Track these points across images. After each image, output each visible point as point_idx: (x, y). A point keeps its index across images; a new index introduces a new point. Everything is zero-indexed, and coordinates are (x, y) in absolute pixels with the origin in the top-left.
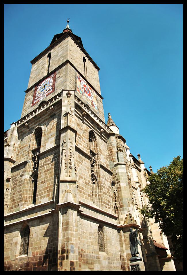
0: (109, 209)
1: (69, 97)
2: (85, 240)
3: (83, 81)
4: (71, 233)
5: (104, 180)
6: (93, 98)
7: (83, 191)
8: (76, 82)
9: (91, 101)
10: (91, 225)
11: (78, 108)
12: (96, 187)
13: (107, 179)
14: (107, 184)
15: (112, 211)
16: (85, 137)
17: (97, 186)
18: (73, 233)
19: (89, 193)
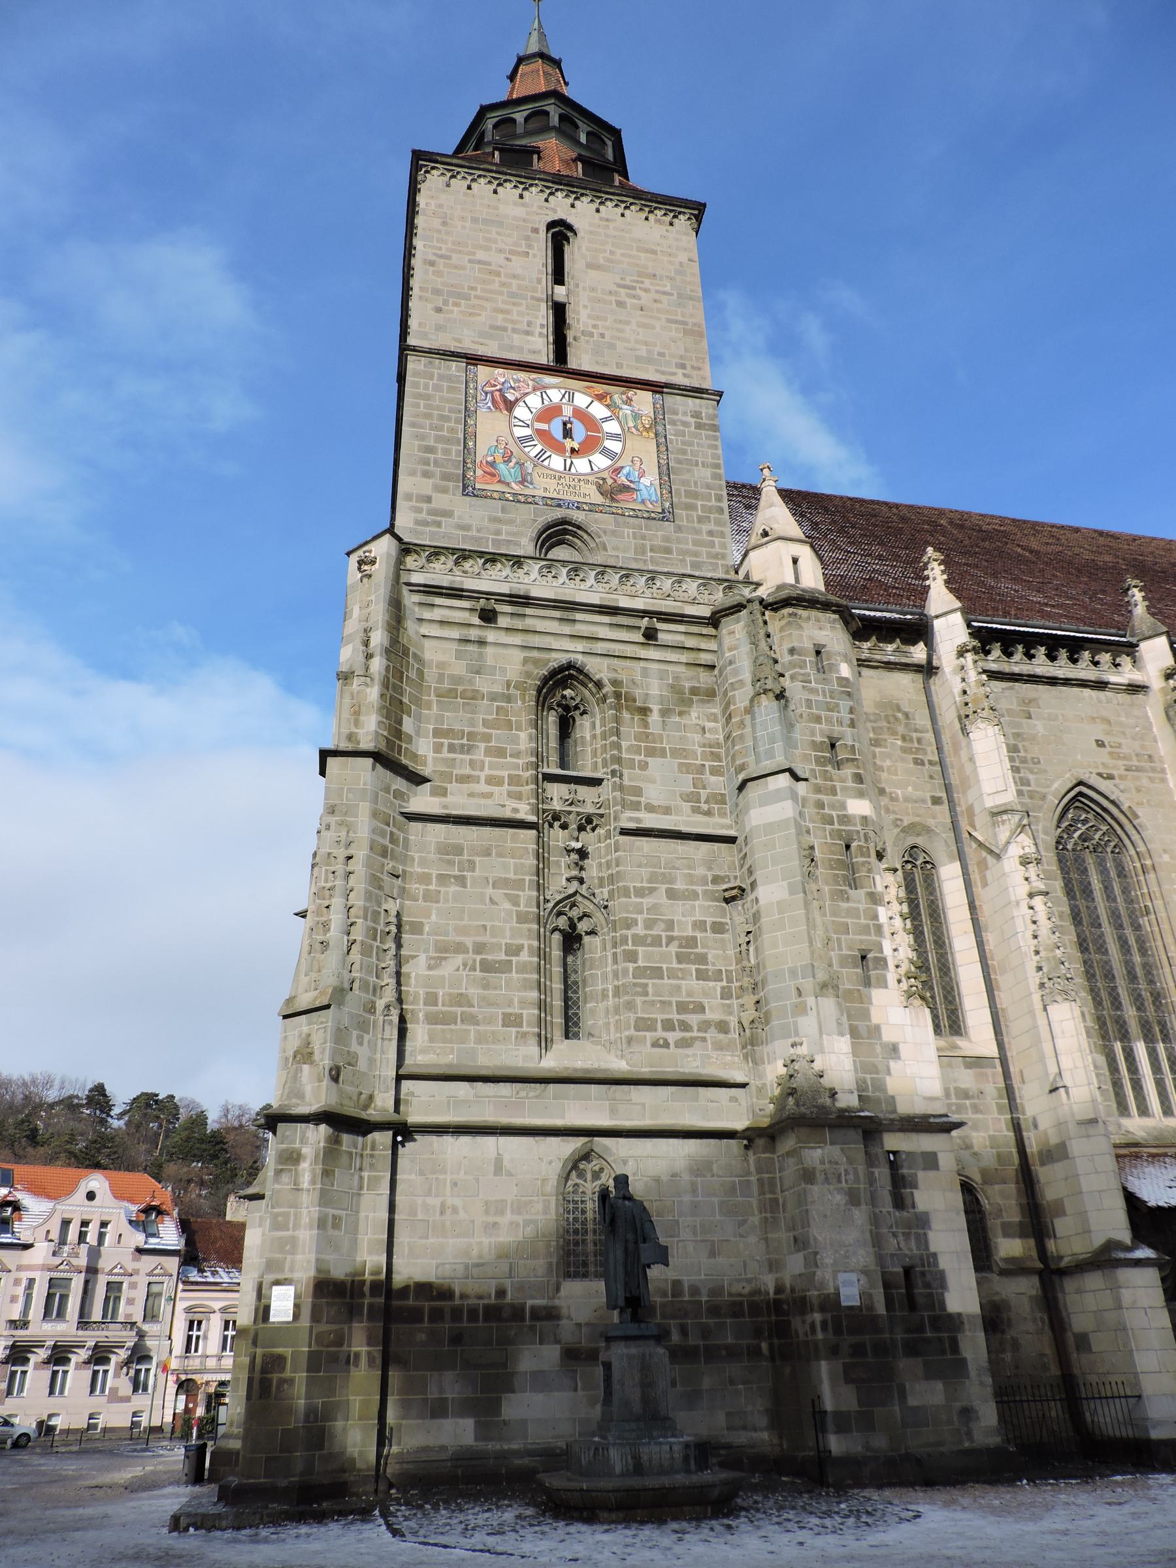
0: (680, 1051)
1: (365, 580)
2: (451, 1241)
3: (535, 389)
4: (280, 1238)
5: (661, 898)
6: (615, 446)
7: (459, 1010)
8: (469, 435)
9: (605, 475)
10: (505, 1163)
11: (438, 601)
12: (605, 949)
13: (680, 885)
14: (676, 919)
15: (714, 1054)
16: (509, 725)
17: (608, 946)
18: (293, 1241)
19: (509, 1010)
